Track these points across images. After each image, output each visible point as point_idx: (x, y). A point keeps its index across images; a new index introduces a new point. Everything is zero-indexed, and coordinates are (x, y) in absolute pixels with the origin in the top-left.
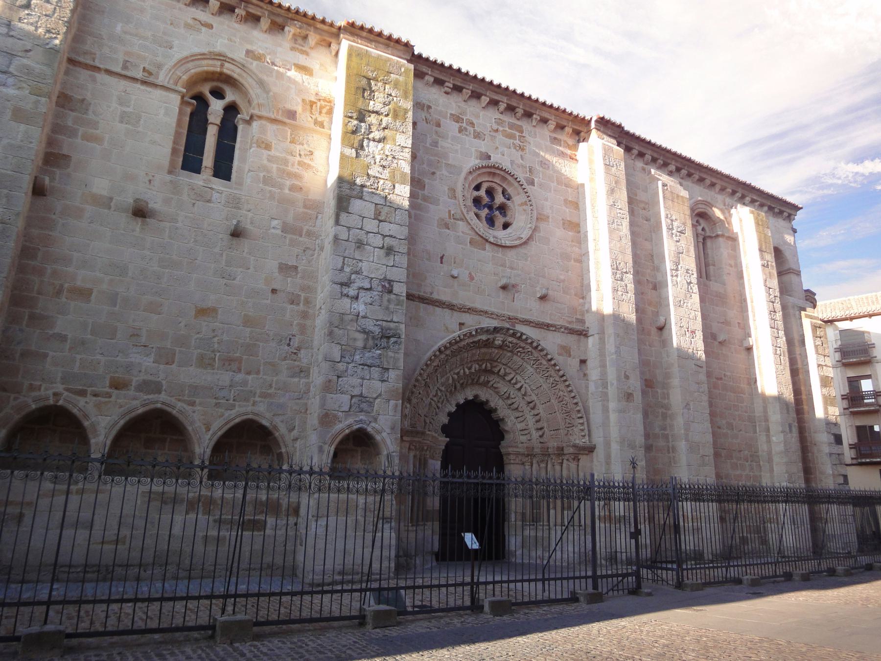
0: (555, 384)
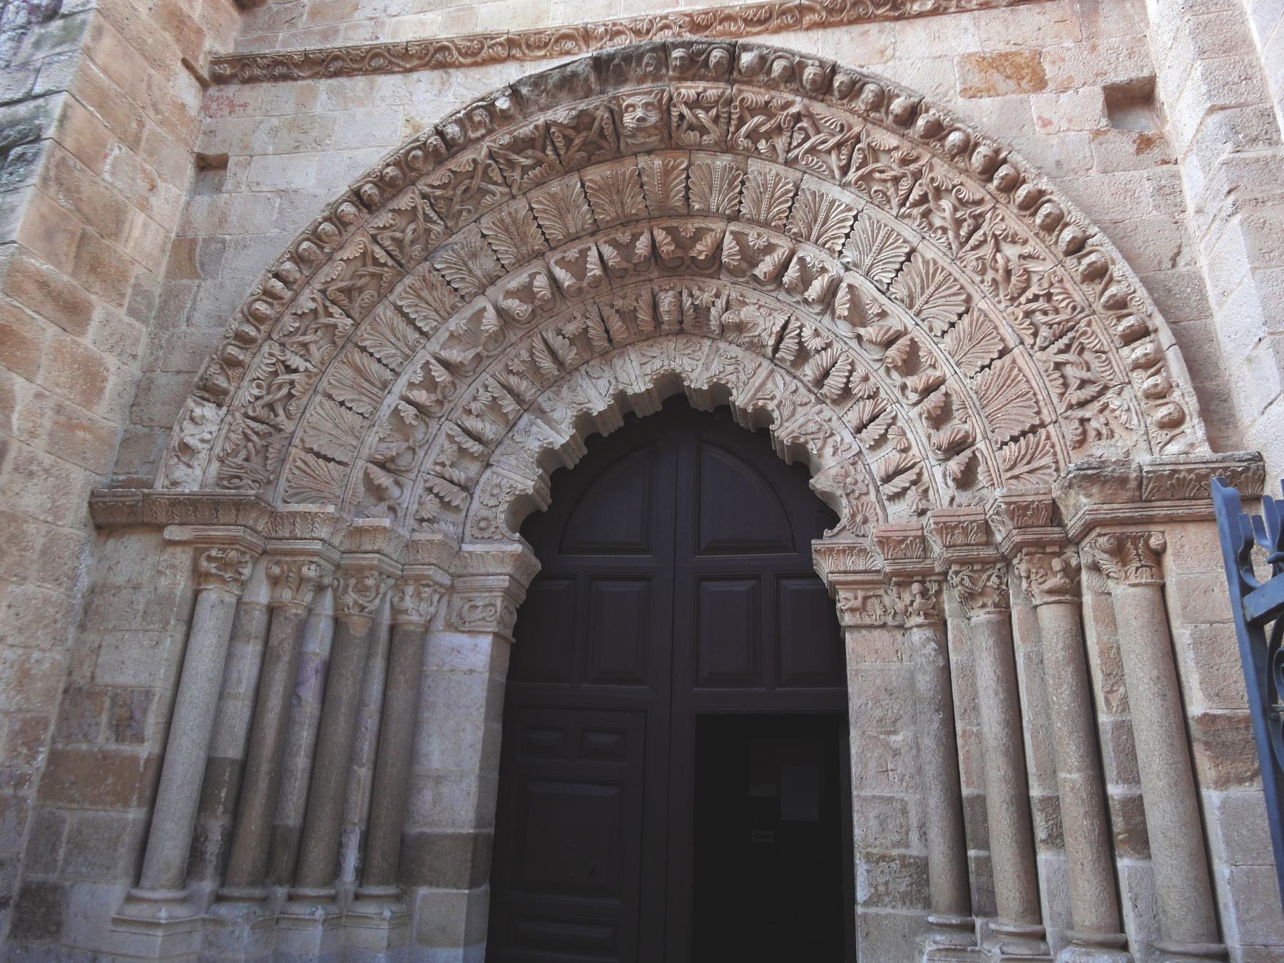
0: (970, 222)
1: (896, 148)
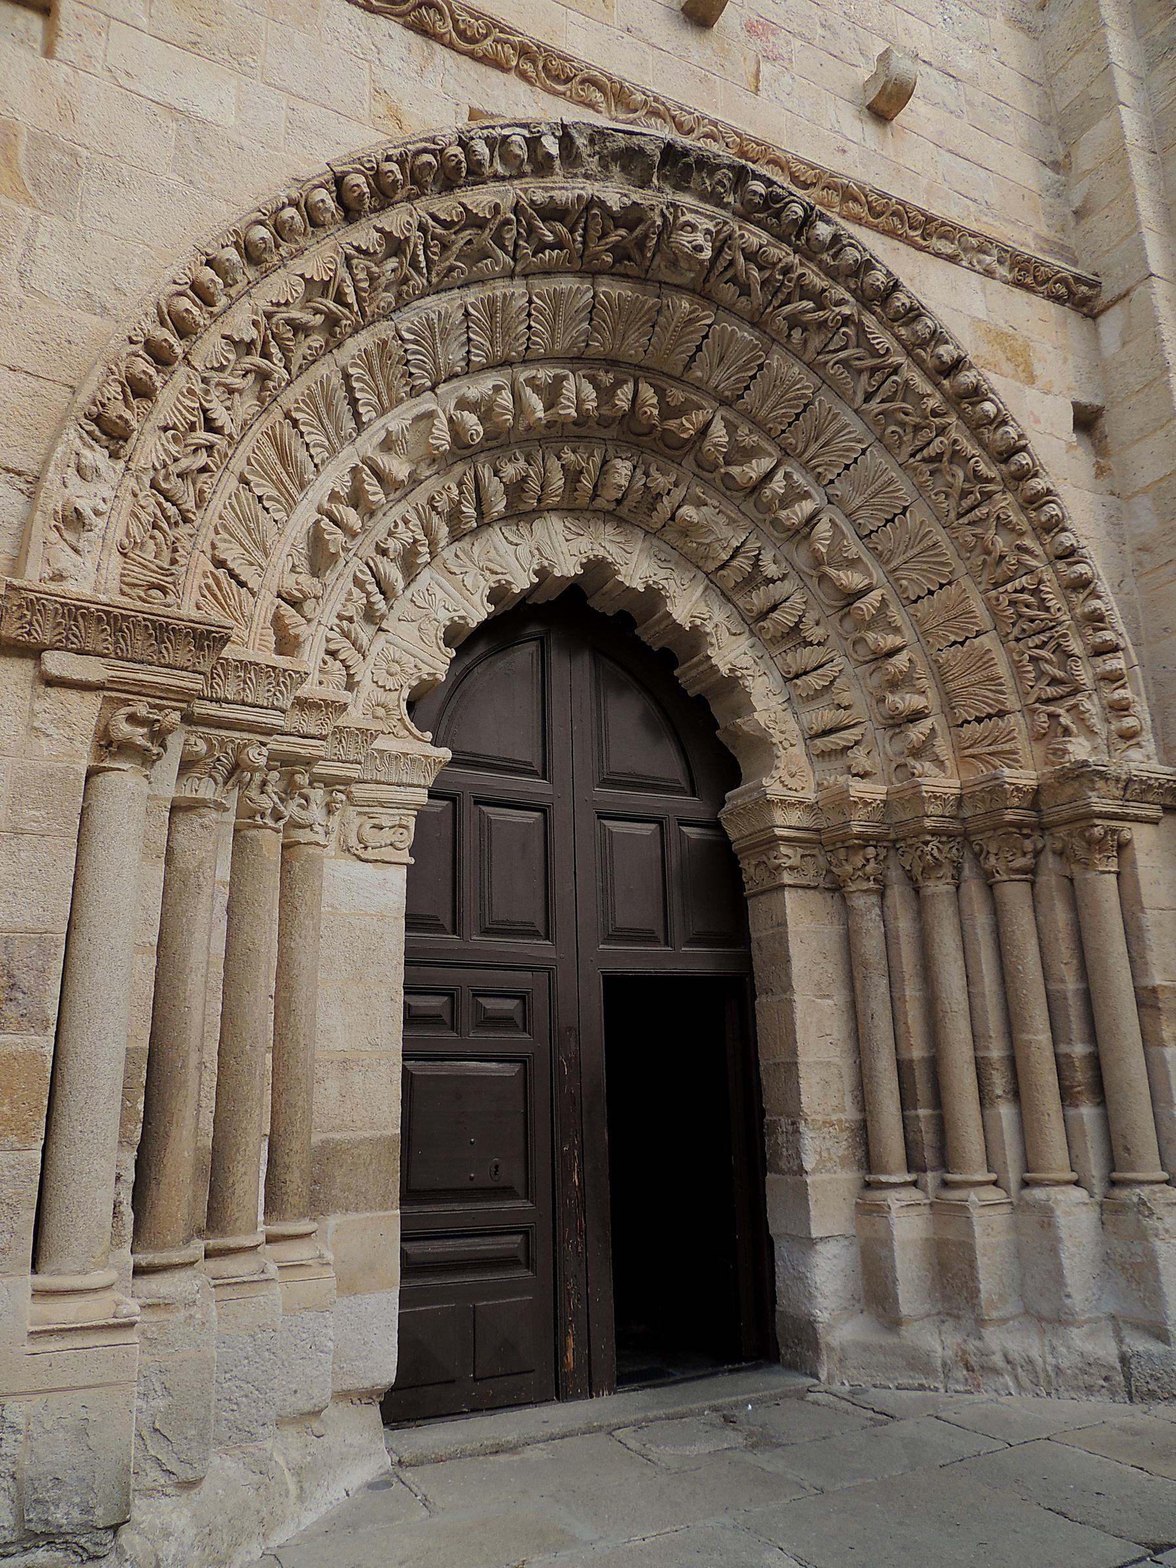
1: (929, 395)
